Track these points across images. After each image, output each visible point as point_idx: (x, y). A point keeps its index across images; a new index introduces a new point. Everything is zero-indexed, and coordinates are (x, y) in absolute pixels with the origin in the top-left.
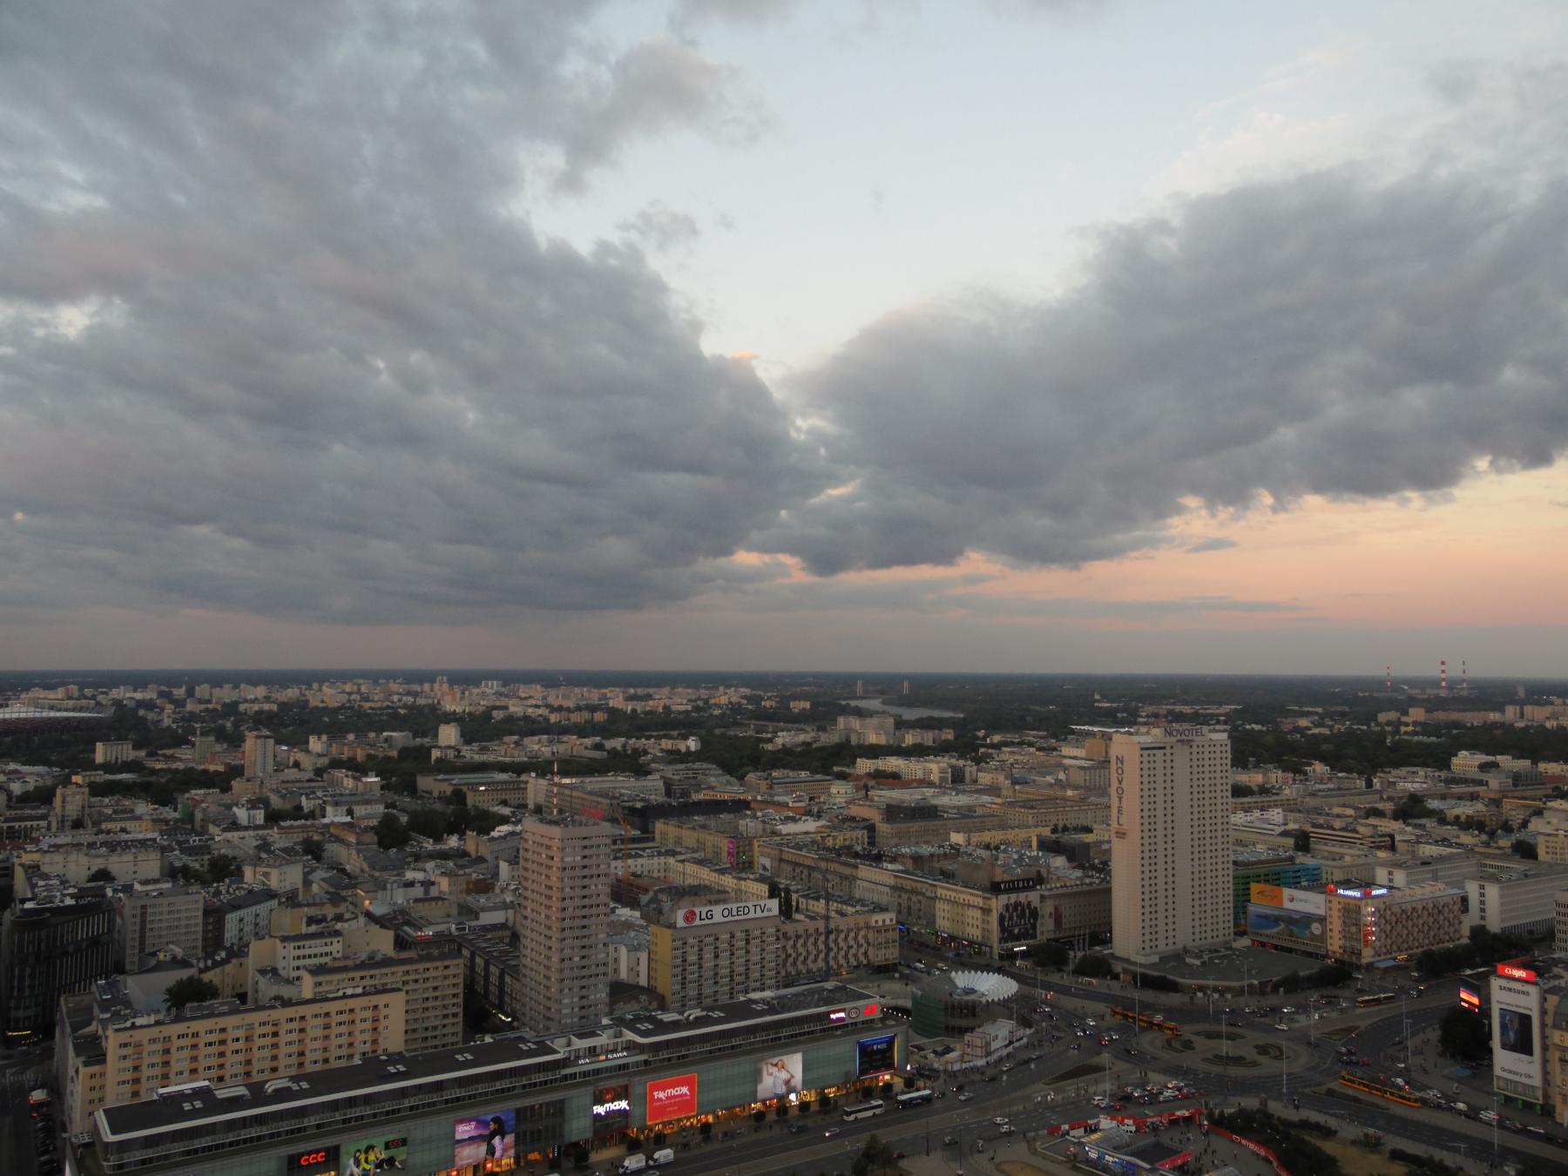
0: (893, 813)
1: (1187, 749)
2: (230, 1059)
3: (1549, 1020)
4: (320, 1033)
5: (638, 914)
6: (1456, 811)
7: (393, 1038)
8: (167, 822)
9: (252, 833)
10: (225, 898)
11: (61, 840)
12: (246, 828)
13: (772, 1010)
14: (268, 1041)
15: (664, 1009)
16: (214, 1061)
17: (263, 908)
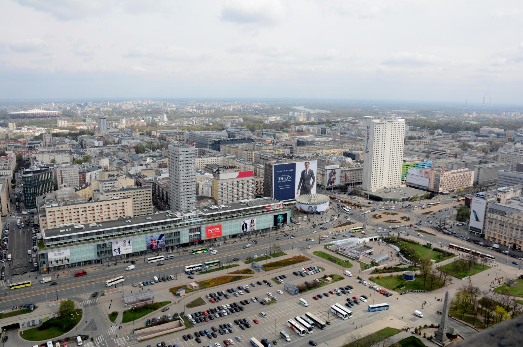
0: (300, 143)
1: (391, 124)
2: (81, 217)
3: (488, 210)
4: (107, 210)
5: (212, 175)
6: (478, 145)
7: (129, 212)
8: (74, 145)
9: (99, 148)
10: (86, 169)
11: (44, 150)
12: (97, 147)
13: (247, 206)
14: (91, 212)
15: (216, 204)
16: (76, 217)
17: (98, 171)
